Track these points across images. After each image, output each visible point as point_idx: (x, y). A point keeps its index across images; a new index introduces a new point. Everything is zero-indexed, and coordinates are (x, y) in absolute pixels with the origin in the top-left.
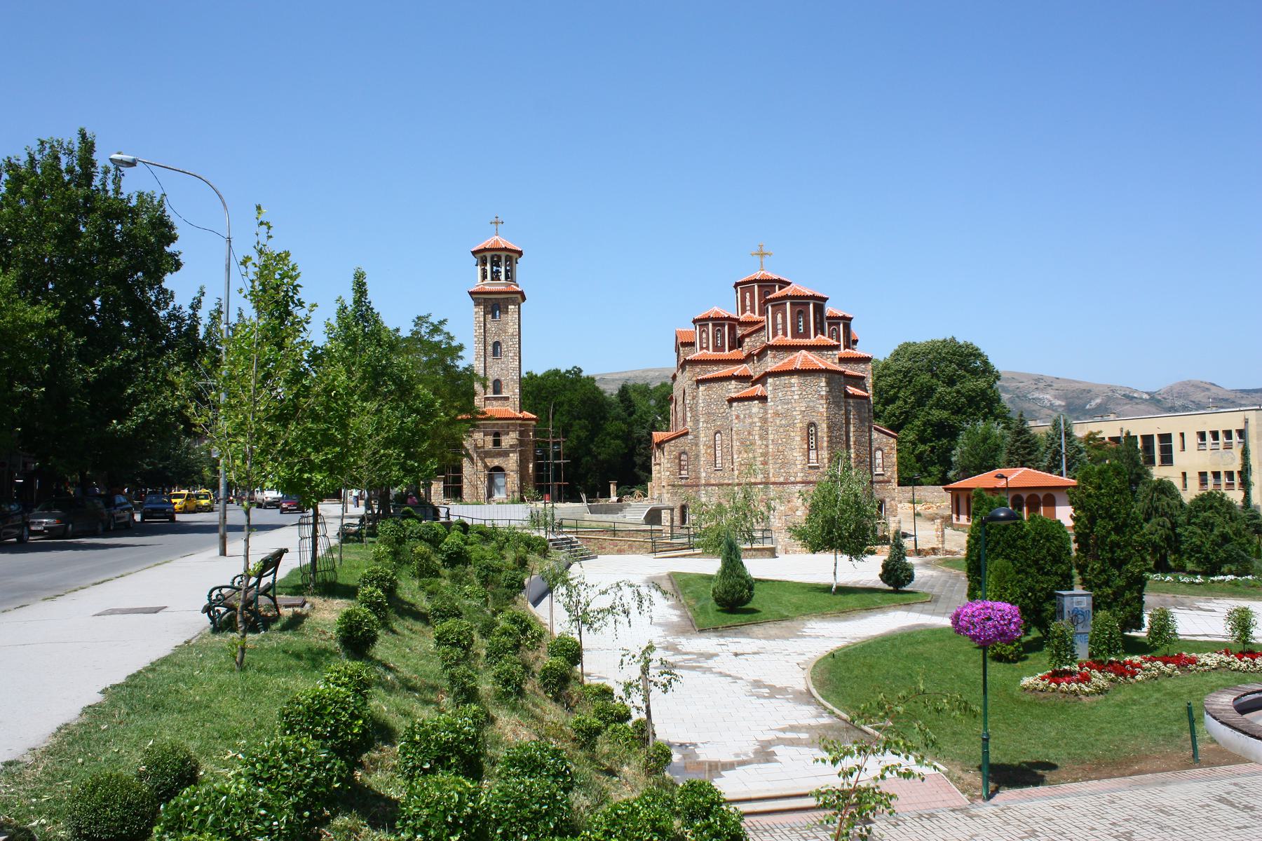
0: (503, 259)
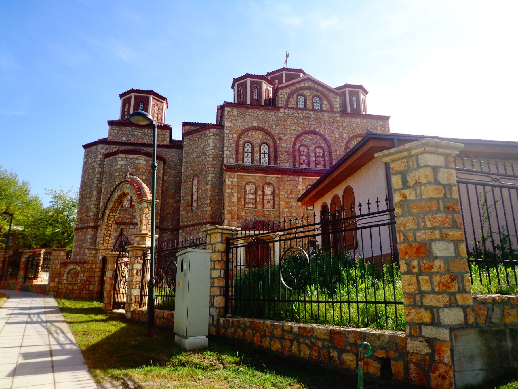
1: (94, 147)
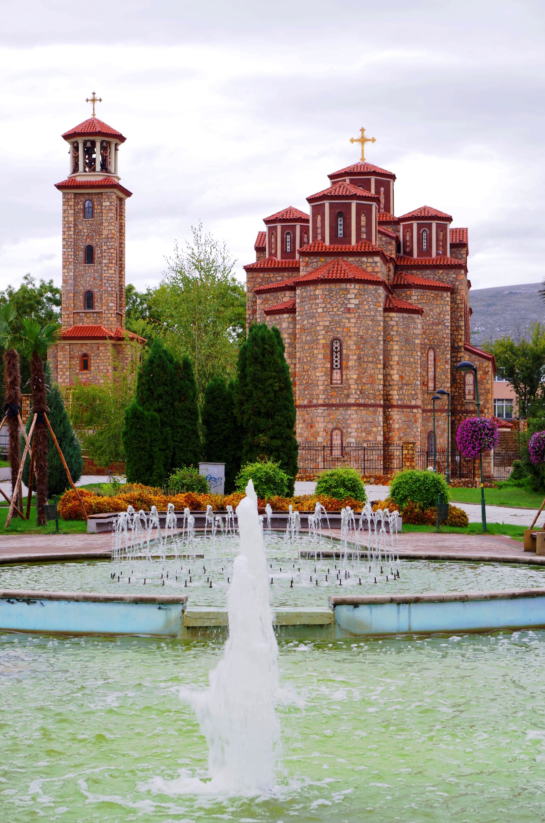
0: (98, 145)
1: (370, 287)
